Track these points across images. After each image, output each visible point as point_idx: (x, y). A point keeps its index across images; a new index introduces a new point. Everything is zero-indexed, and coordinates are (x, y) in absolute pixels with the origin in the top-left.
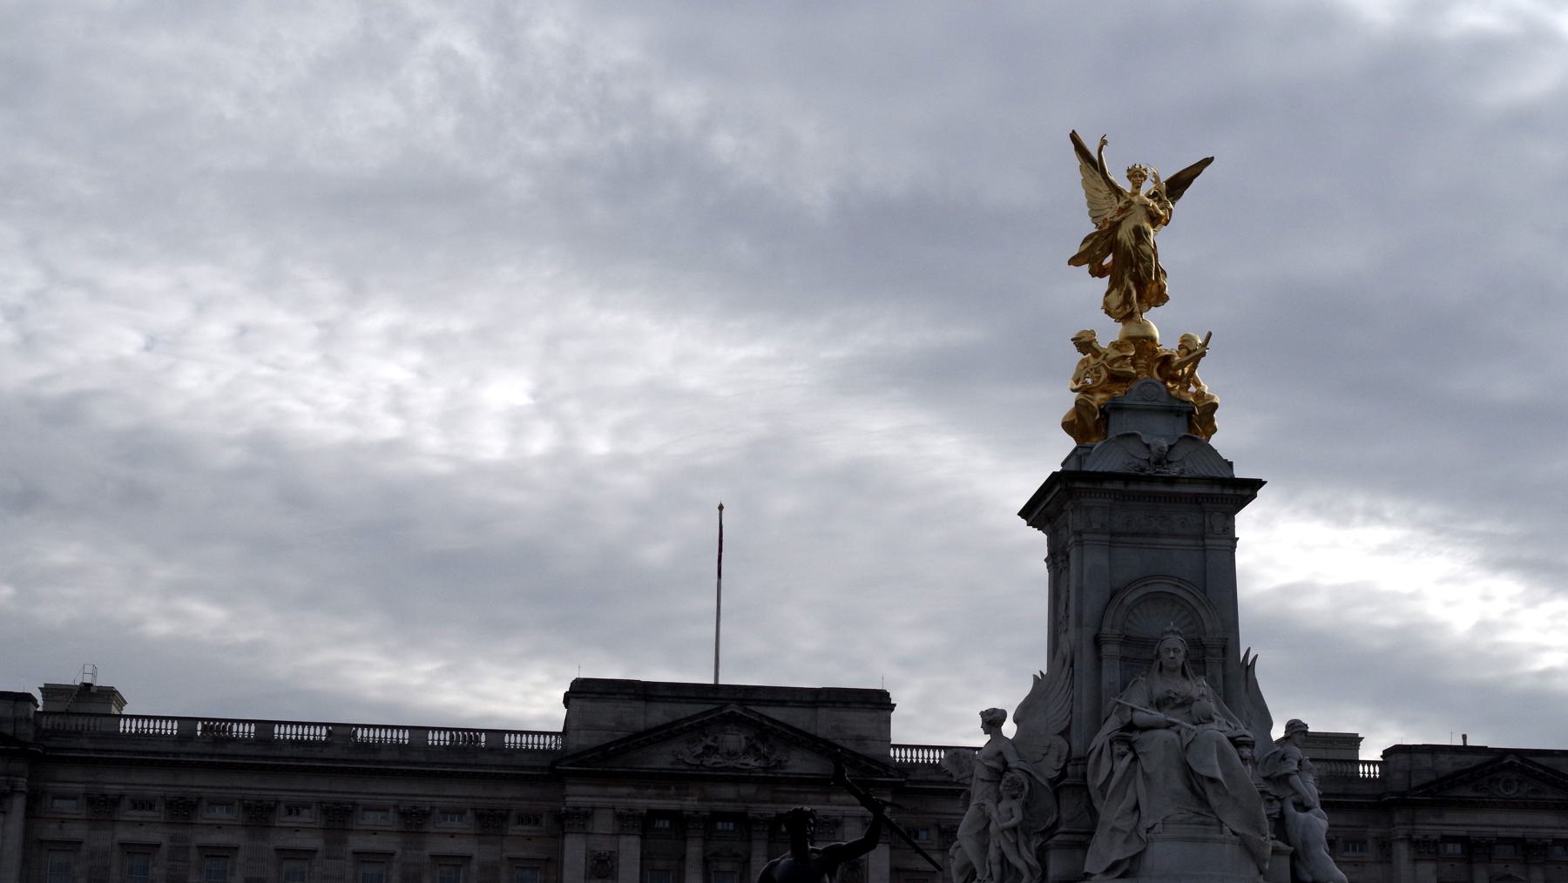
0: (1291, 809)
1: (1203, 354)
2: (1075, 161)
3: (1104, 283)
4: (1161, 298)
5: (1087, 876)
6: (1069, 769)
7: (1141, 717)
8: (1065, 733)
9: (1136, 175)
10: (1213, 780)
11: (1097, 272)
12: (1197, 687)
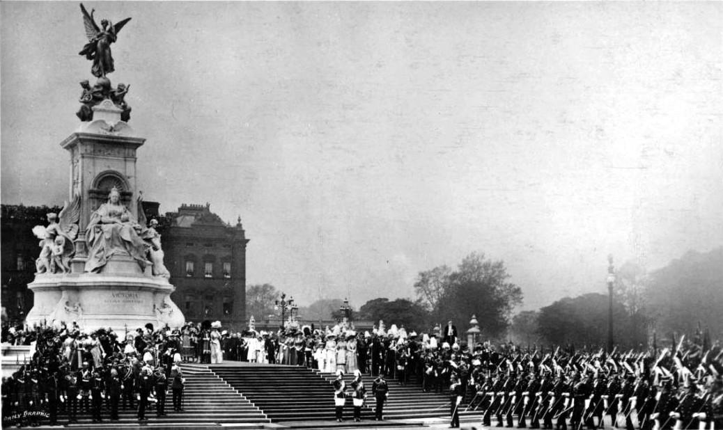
0: (152, 250)
1: (127, 92)
2: (82, 15)
3: (91, 62)
4: (112, 70)
5: (87, 272)
6: (79, 236)
7: (104, 219)
8: (77, 223)
9: (105, 23)
10: (129, 242)
11: (90, 58)
12: (120, 209)
